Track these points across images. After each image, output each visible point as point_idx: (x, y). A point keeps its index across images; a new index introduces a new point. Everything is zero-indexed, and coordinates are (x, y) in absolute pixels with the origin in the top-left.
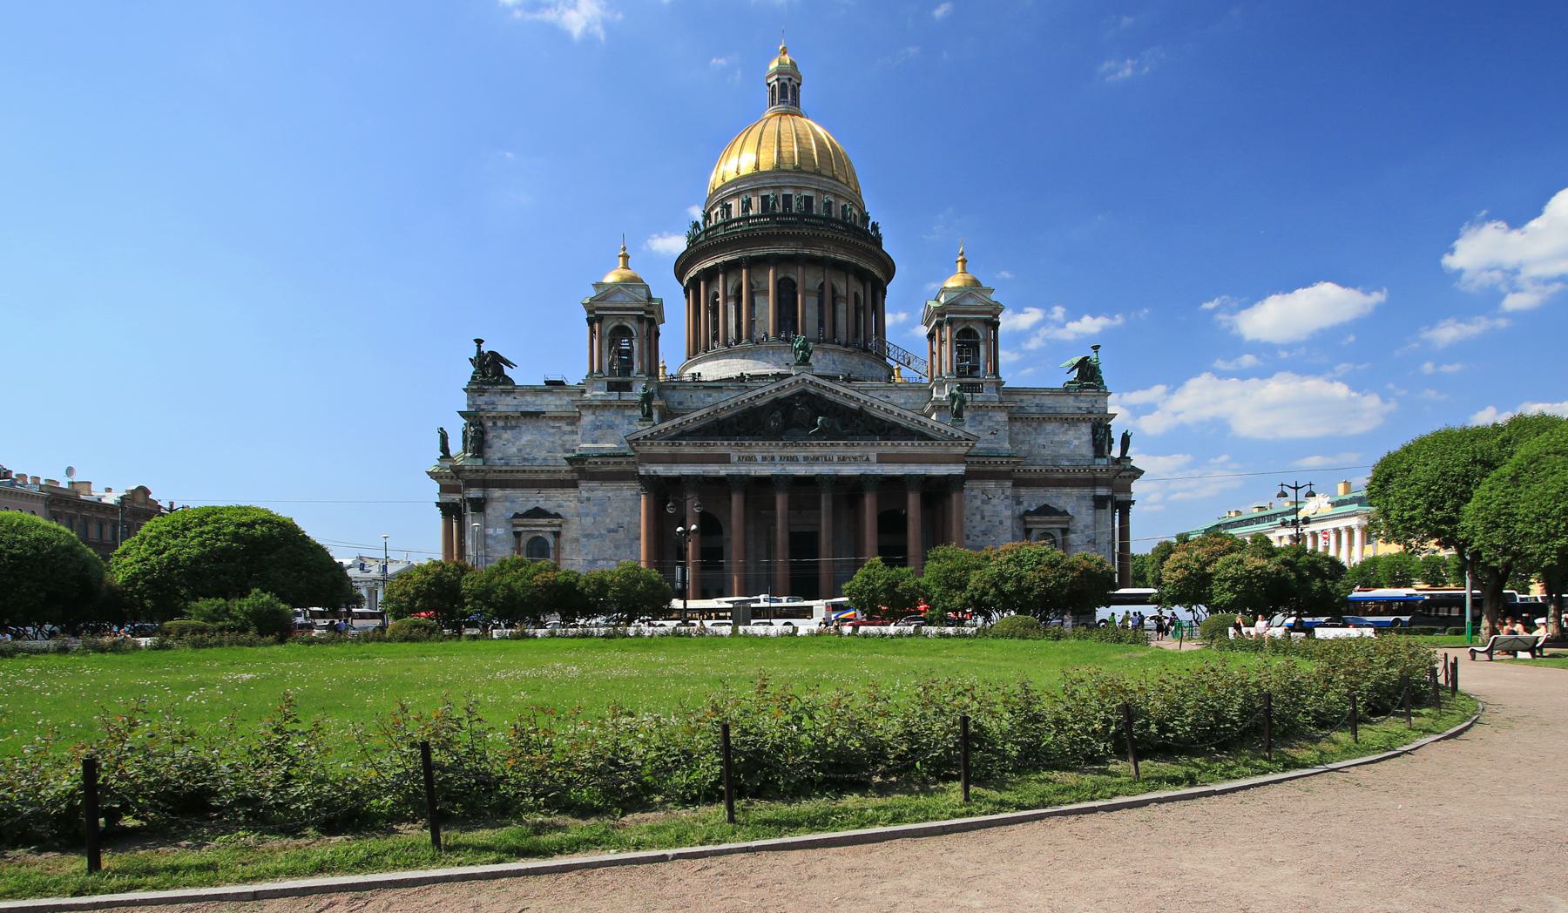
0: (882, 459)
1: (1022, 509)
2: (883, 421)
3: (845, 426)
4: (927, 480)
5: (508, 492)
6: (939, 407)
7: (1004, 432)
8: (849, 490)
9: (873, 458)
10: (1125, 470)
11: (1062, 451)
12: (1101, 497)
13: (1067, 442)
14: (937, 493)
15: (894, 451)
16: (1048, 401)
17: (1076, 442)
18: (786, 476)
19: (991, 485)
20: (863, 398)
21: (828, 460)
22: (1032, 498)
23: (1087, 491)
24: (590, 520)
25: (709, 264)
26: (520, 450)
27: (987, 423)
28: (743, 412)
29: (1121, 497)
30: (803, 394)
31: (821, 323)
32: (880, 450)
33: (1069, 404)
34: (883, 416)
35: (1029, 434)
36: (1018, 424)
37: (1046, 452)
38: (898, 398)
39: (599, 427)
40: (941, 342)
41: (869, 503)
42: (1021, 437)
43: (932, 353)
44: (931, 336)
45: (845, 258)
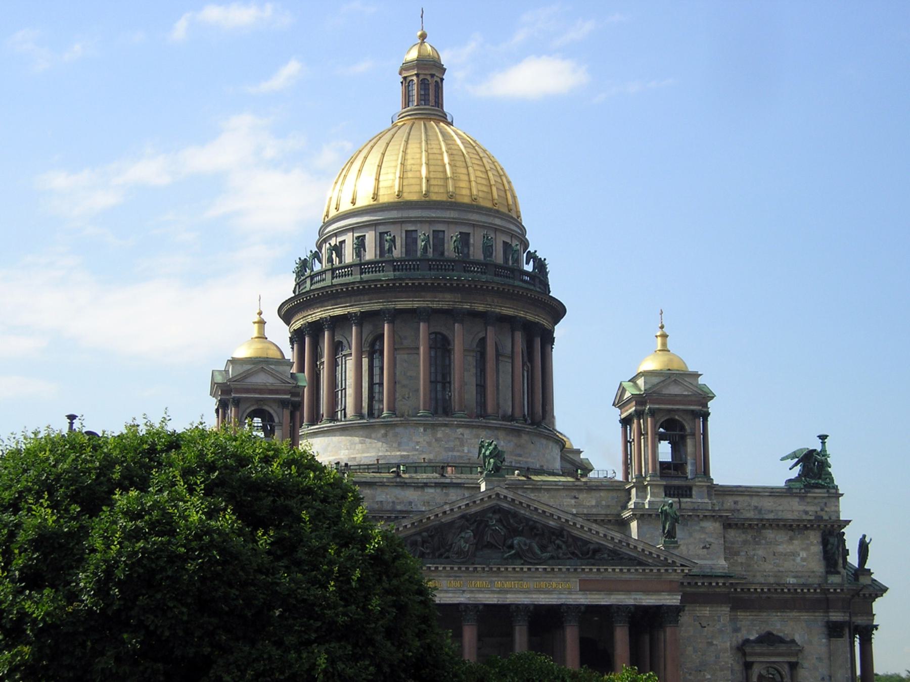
0: (585, 587)
2: (586, 542)
3: (543, 548)
4: (638, 608)
6: (642, 516)
7: (718, 545)
8: (545, 620)
9: (574, 583)
10: (866, 586)
11: (788, 565)
13: (794, 554)
14: (647, 623)
15: (599, 577)
16: (767, 503)
18: (476, 606)
19: (706, 611)
20: (564, 517)
22: (751, 627)
23: (819, 616)
25: (339, 312)
28: (427, 530)
29: (860, 620)
30: (496, 510)
31: (481, 387)
32: (583, 576)
33: (794, 509)
34: (585, 536)
35: (745, 542)
36: (732, 534)
37: (768, 567)
38: (589, 501)
40: (640, 434)
41: (571, 635)
43: (626, 442)
44: (626, 422)
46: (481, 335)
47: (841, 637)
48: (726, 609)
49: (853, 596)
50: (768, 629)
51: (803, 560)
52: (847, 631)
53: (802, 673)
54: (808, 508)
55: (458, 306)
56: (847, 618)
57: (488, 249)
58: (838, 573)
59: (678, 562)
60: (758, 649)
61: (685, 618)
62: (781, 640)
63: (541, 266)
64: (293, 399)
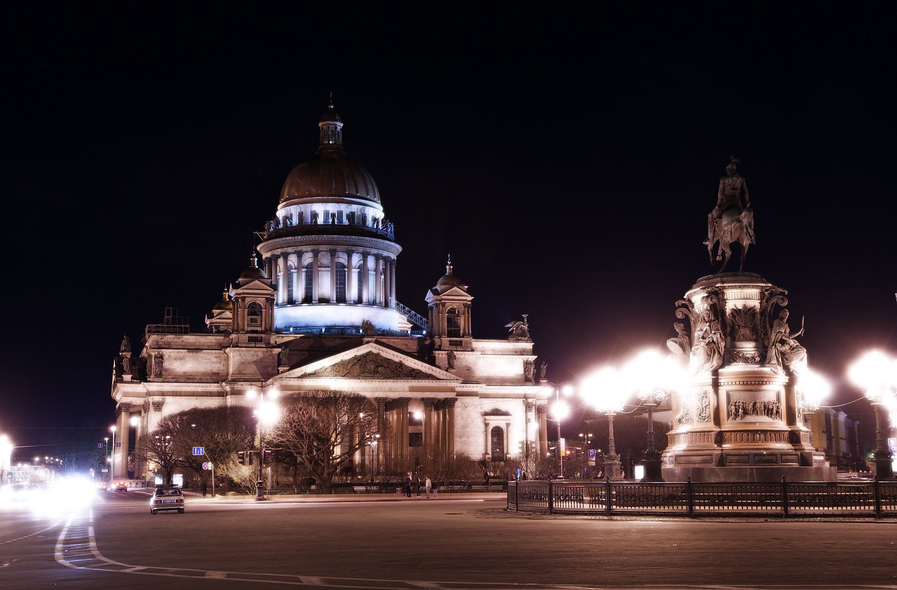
2: (413, 370)
9: (407, 388)
53: (511, 428)
60: (492, 417)
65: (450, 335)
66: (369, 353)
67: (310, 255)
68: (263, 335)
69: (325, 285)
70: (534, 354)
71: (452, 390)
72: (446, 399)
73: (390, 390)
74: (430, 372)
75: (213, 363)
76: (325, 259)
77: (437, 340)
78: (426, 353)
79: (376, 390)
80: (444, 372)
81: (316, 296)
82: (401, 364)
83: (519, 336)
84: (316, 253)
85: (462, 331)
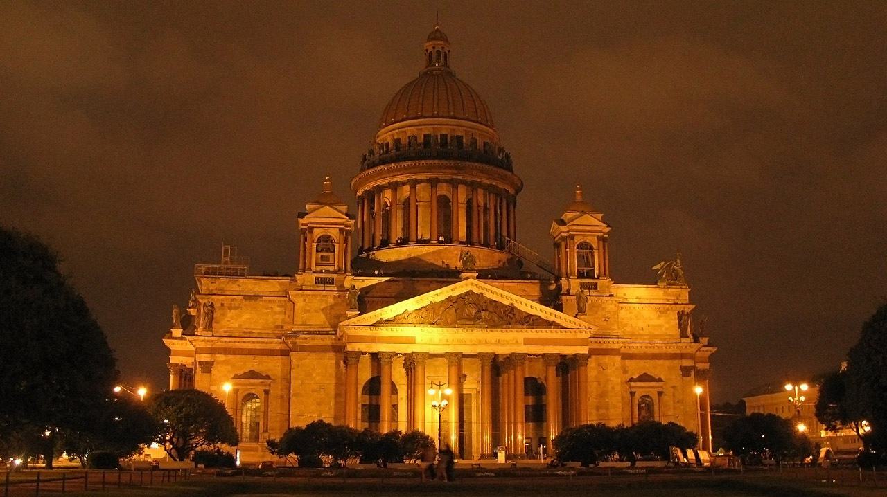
0: (528, 342)
1: (628, 377)
2: (530, 316)
5: (230, 357)
9: (521, 341)
12: (686, 367)
17: (666, 326)
21: (487, 344)
24: (300, 382)
26: (240, 325)
27: (600, 313)
39: (308, 311)
42: (625, 322)
45: (488, 182)
46: (471, 196)
47: (689, 375)
48: (618, 358)
49: (697, 351)
50: (644, 372)
51: (667, 329)
52: (692, 373)
53: (665, 398)
54: (669, 298)
55: (454, 177)
56: (693, 365)
57: (473, 142)
58: (688, 337)
59: (587, 328)
60: (639, 384)
61: (592, 363)
62: (651, 379)
63: (508, 157)
64: (347, 228)
65: (581, 276)
66: (470, 293)
67: (407, 188)
68: (335, 276)
69: (424, 224)
70: (690, 303)
71: (583, 343)
72: (576, 355)
73: (498, 343)
74: (552, 319)
75: (276, 313)
76: (423, 192)
77: (563, 282)
78: (552, 299)
79: (479, 343)
80: (572, 319)
81: (413, 237)
82: (512, 308)
83: (673, 279)
84: (414, 183)
85: (596, 272)
